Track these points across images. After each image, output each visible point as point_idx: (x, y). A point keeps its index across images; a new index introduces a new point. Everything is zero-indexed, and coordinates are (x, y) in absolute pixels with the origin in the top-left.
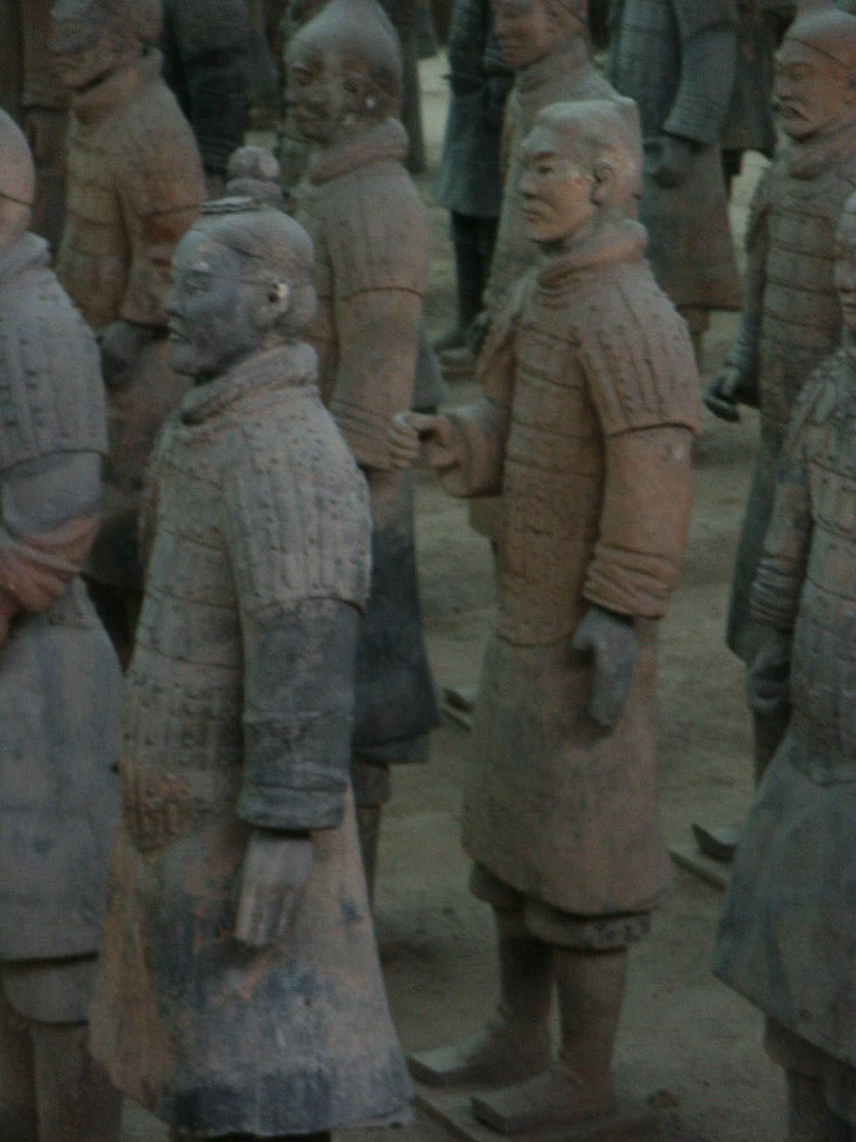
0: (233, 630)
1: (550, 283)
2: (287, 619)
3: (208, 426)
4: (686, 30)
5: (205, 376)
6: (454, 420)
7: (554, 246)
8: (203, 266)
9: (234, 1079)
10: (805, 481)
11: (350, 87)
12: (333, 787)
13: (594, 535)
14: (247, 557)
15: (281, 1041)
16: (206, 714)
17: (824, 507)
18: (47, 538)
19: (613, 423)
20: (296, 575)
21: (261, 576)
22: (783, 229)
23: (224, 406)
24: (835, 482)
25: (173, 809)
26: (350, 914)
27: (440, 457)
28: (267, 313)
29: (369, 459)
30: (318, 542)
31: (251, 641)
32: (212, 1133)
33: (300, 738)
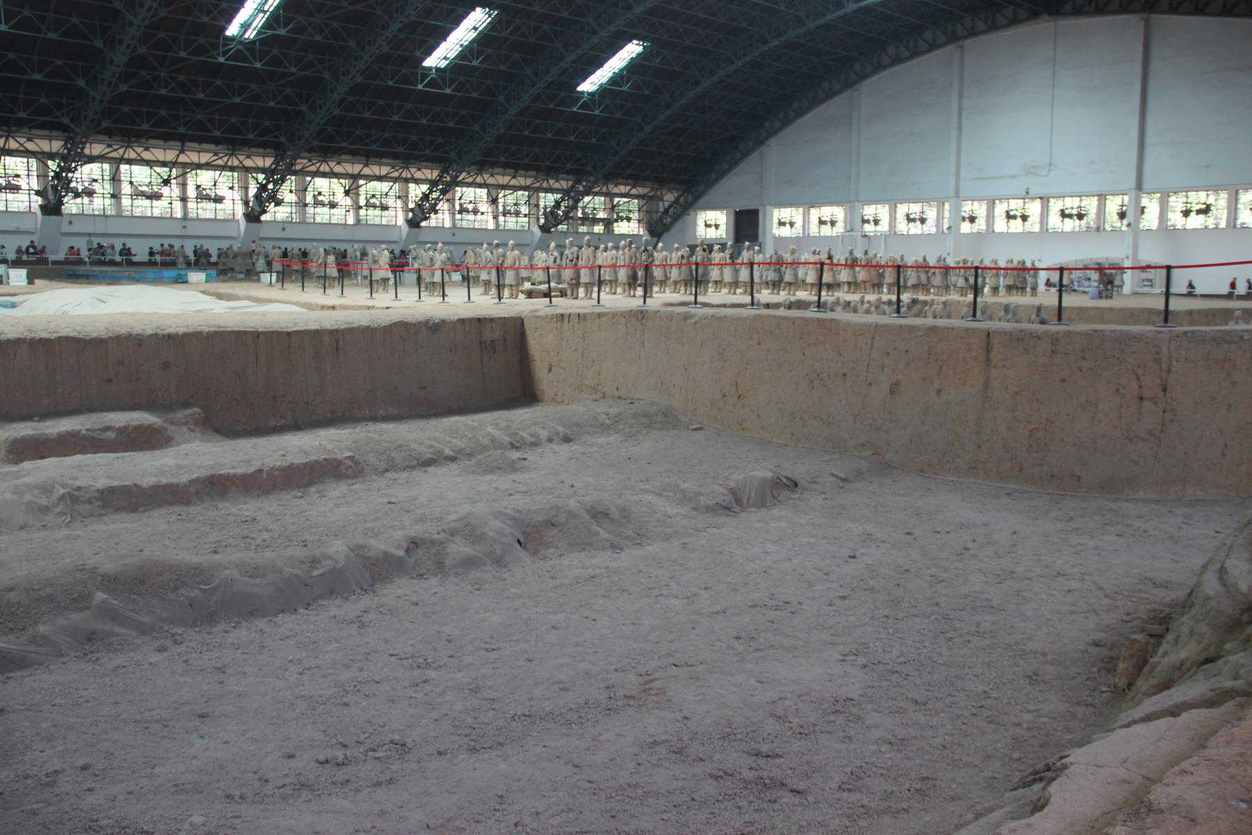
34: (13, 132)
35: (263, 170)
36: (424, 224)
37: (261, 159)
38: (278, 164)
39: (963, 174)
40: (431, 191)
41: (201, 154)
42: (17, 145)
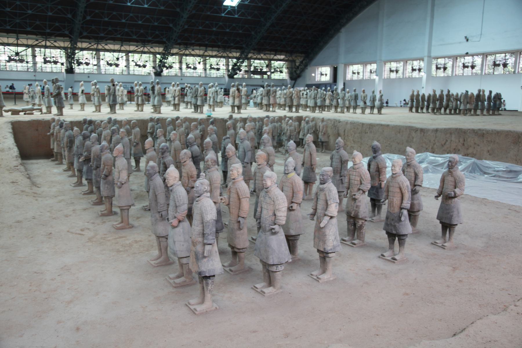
0: (203, 223)
1: (233, 183)
2: (208, 222)
3: (199, 202)
4: (246, 151)
5: (199, 197)
6: (224, 197)
7: (234, 179)
9: (205, 270)
10: (261, 203)
11: (212, 163)
12: (214, 239)
13: (239, 209)
15: (209, 265)
16: (200, 232)
17: (263, 206)
18: (182, 213)
19: (241, 197)
21: (205, 218)
22: (257, 174)
24: (264, 203)
26: (216, 252)
27: (223, 201)
28: (205, 190)
29: (215, 201)
30: (211, 214)
31: (204, 224)
34: (48, 38)
35: (159, 54)
36: (235, 76)
37: (26, 40)
38: (165, 51)
39: (434, 43)
40: (237, 62)
41: (28, 40)
42: (50, 44)
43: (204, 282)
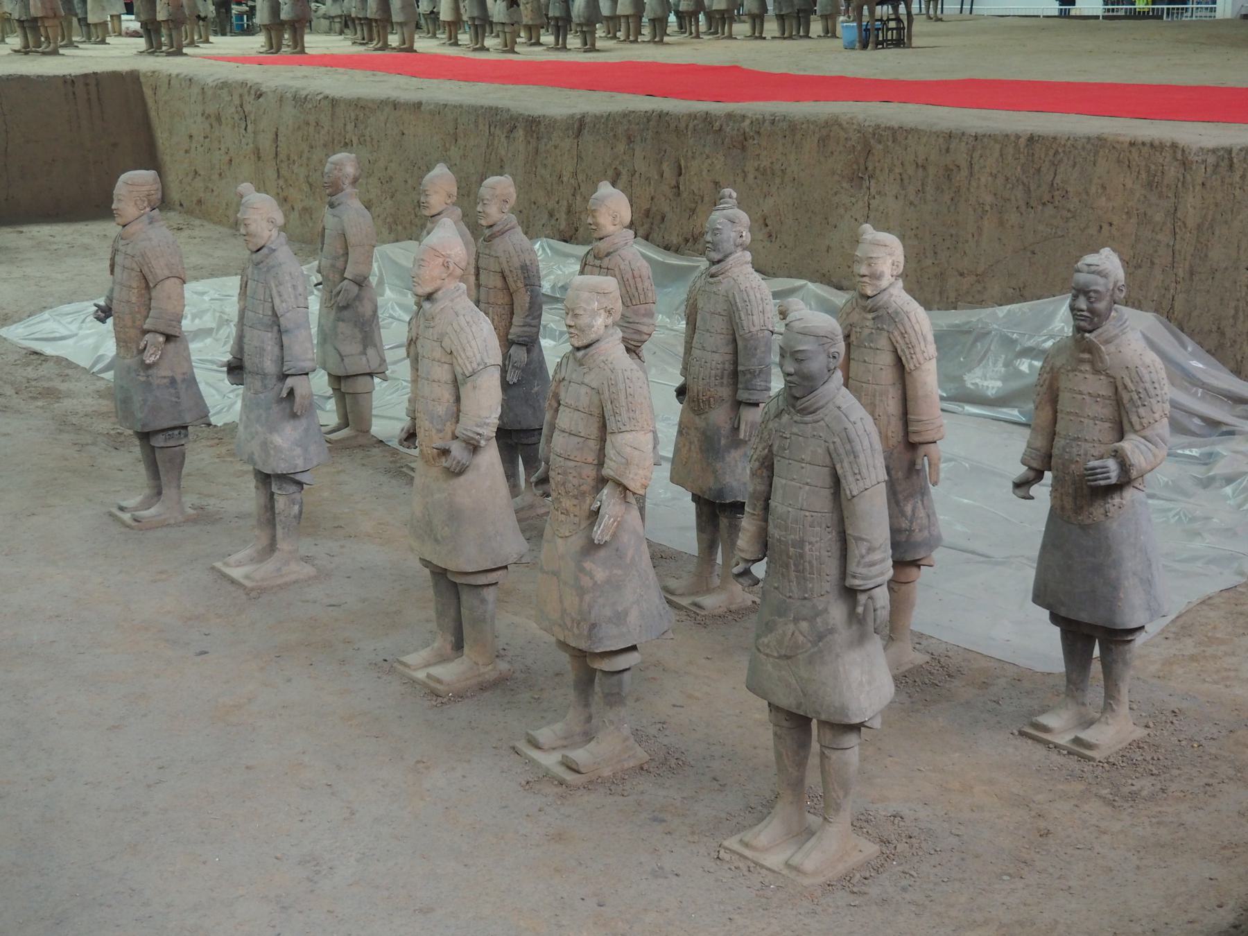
3: (720, 277)
8: (719, 226)
9: (735, 484)
14: (740, 318)
20: (756, 322)
21: (745, 323)
23: (726, 271)
25: (712, 399)
28: (739, 241)
32: (728, 502)
33: (758, 375)
43: (724, 522)
